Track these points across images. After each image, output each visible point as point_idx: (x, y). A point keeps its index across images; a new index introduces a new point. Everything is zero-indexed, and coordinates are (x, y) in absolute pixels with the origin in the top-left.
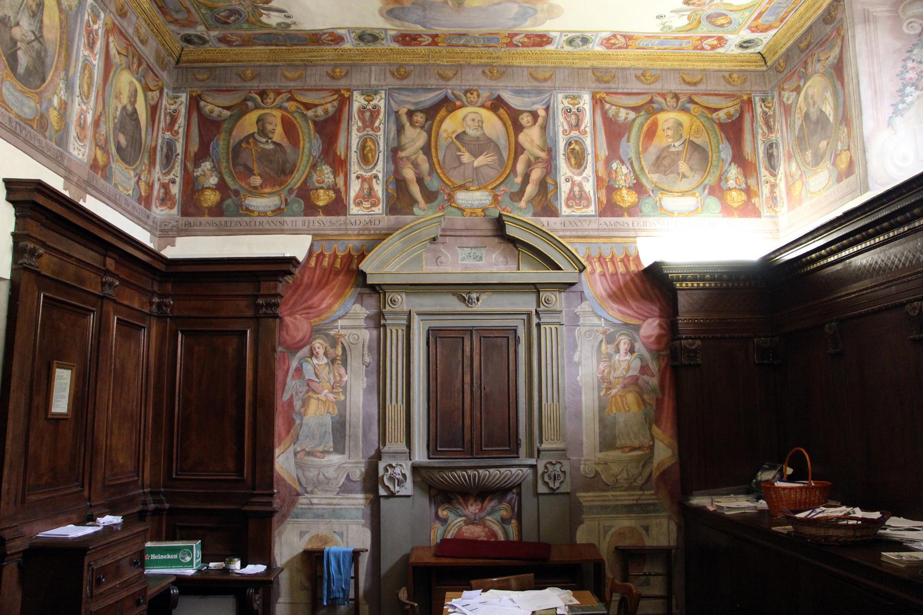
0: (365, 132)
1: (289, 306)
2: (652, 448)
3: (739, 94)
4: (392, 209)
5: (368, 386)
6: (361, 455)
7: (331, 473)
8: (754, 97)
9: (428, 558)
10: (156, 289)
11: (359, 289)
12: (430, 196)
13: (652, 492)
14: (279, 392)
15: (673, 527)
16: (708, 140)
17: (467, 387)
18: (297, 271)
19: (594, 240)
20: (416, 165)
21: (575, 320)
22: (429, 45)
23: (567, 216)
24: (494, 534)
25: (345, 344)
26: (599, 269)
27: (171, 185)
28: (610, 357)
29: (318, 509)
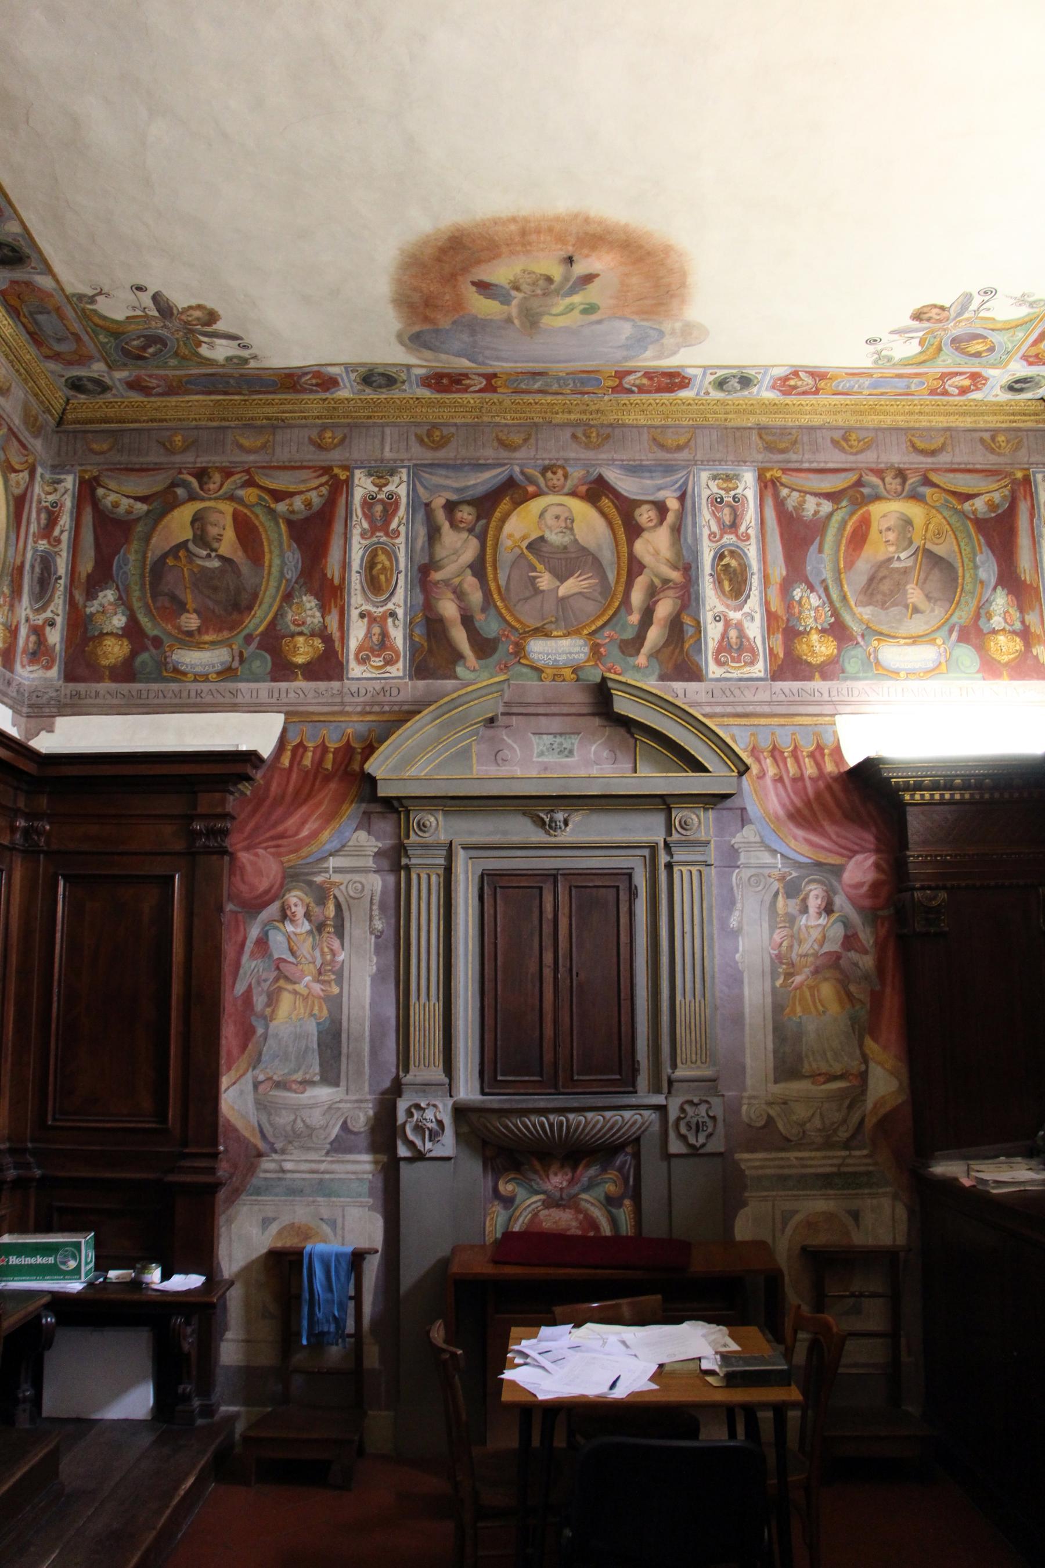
0: (375, 539)
1: (246, 834)
2: (864, 1076)
3: (1008, 469)
4: (420, 669)
5: (378, 970)
6: (367, 1089)
7: (316, 1118)
8: (1034, 473)
9: (481, 1266)
10: (21, 804)
11: (364, 806)
12: (484, 647)
13: (865, 1152)
14: (228, 980)
15: (901, 1212)
16: (956, 548)
17: (548, 973)
18: (259, 775)
19: (763, 721)
20: (460, 595)
21: (731, 857)
22: (480, 391)
23: (718, 680)
24: (594, 1225)
25: (341, 899)
26: (771, 771)
27: (48, 629)
28: (791, 920)
29: (294, 1180)
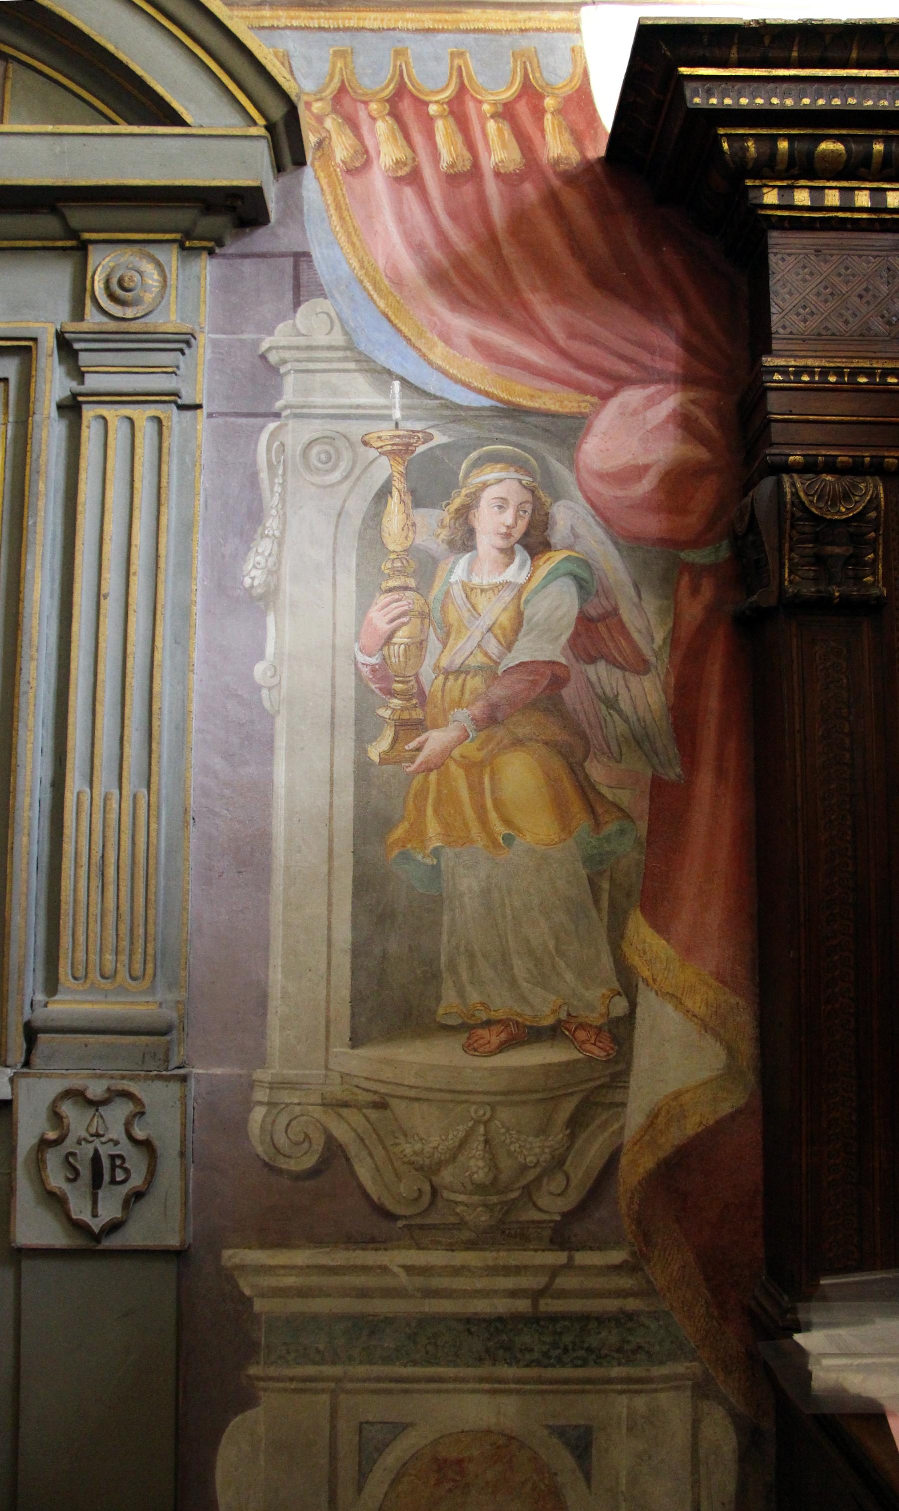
13: (617, 1256)
